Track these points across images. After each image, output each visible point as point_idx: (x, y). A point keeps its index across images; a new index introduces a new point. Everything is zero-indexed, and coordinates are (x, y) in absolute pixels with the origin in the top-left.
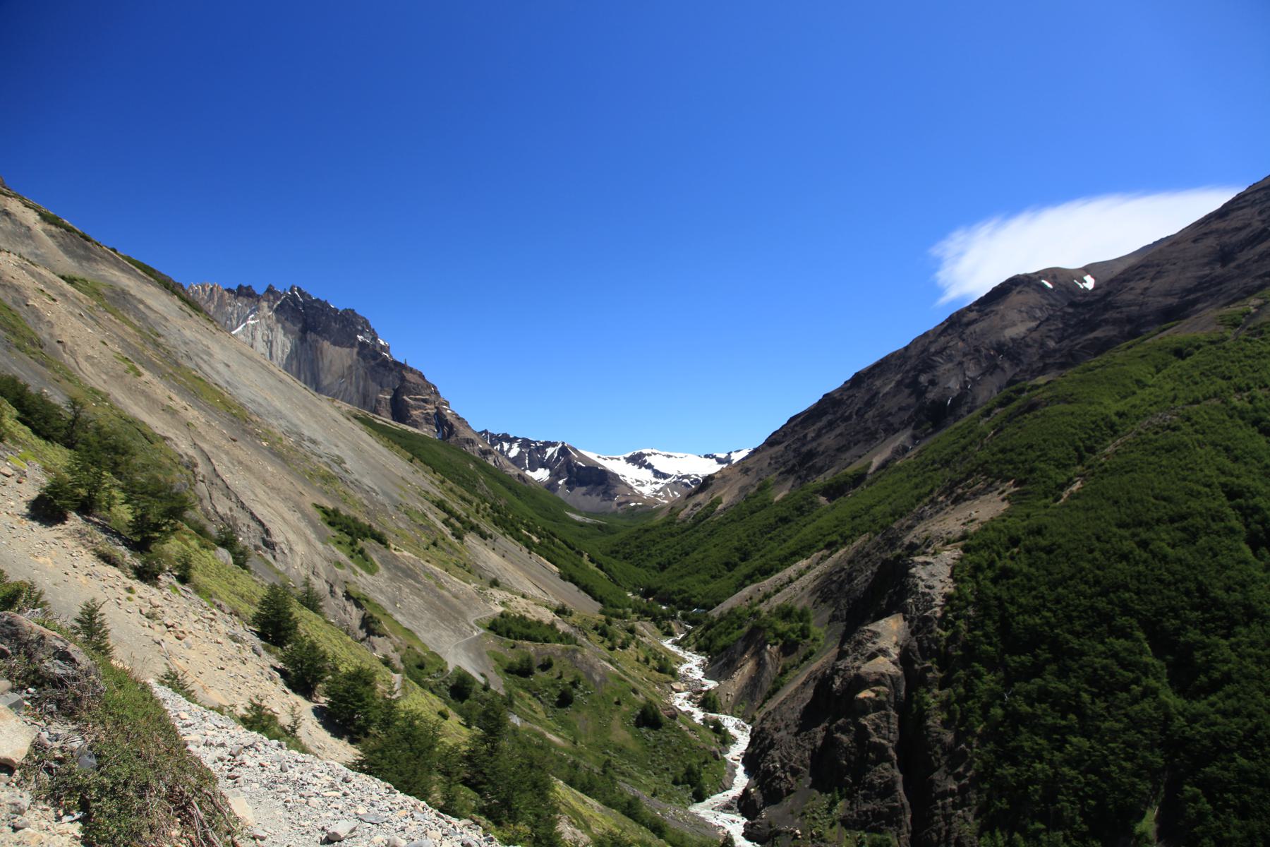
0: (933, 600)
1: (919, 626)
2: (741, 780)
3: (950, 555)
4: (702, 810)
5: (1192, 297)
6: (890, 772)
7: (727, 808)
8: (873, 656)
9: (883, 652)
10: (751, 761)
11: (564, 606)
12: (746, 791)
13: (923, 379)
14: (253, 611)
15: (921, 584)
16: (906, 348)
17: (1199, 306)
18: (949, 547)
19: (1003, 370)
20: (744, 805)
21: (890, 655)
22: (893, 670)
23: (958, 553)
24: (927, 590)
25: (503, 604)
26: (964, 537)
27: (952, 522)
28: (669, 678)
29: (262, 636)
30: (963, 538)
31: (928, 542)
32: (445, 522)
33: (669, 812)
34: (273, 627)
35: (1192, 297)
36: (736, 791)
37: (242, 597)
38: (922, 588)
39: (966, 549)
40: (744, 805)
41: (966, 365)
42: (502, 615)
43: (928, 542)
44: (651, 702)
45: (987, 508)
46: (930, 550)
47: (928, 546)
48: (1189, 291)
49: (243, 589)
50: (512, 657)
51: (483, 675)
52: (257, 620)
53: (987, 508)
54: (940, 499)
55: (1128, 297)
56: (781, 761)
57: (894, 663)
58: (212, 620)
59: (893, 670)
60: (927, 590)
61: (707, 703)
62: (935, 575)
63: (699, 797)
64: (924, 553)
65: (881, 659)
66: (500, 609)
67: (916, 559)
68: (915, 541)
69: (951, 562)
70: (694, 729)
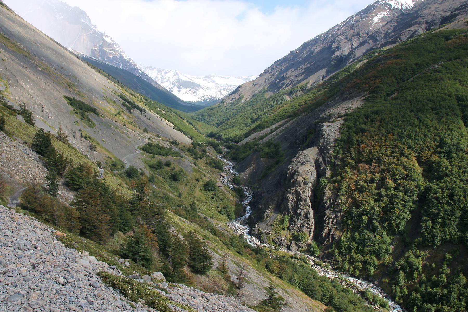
3: (340, 122)
5: (456, 12)
11: (175, 141)
13: (334, 46)
14: (31, 141)
16: (328, 32)
17: (459, 17)
19: (369, 43)
23: (342, 122)
24: (328, 137)
25: (149, 139)
26: (346, 115)
27: (341, 109)
28: (220, 171)
30: (345, 116)
31: (330, 117)
32: (124, 104)
35: (456, 12)
41: (353, 40)
42: (148, 144)
43: (330, 117)
45: (356, 104)
46: (331, 120)
47: (330, 119)
48: (456, 10)
50: (153, 161)
51: (141, 169)
53: (356, 104)
54: (337, 98)
55: (427, 11)
62: (331, 131)
64: (328, 122)
66: (147, 141)
67: (325, 123)
68: (325, 116)
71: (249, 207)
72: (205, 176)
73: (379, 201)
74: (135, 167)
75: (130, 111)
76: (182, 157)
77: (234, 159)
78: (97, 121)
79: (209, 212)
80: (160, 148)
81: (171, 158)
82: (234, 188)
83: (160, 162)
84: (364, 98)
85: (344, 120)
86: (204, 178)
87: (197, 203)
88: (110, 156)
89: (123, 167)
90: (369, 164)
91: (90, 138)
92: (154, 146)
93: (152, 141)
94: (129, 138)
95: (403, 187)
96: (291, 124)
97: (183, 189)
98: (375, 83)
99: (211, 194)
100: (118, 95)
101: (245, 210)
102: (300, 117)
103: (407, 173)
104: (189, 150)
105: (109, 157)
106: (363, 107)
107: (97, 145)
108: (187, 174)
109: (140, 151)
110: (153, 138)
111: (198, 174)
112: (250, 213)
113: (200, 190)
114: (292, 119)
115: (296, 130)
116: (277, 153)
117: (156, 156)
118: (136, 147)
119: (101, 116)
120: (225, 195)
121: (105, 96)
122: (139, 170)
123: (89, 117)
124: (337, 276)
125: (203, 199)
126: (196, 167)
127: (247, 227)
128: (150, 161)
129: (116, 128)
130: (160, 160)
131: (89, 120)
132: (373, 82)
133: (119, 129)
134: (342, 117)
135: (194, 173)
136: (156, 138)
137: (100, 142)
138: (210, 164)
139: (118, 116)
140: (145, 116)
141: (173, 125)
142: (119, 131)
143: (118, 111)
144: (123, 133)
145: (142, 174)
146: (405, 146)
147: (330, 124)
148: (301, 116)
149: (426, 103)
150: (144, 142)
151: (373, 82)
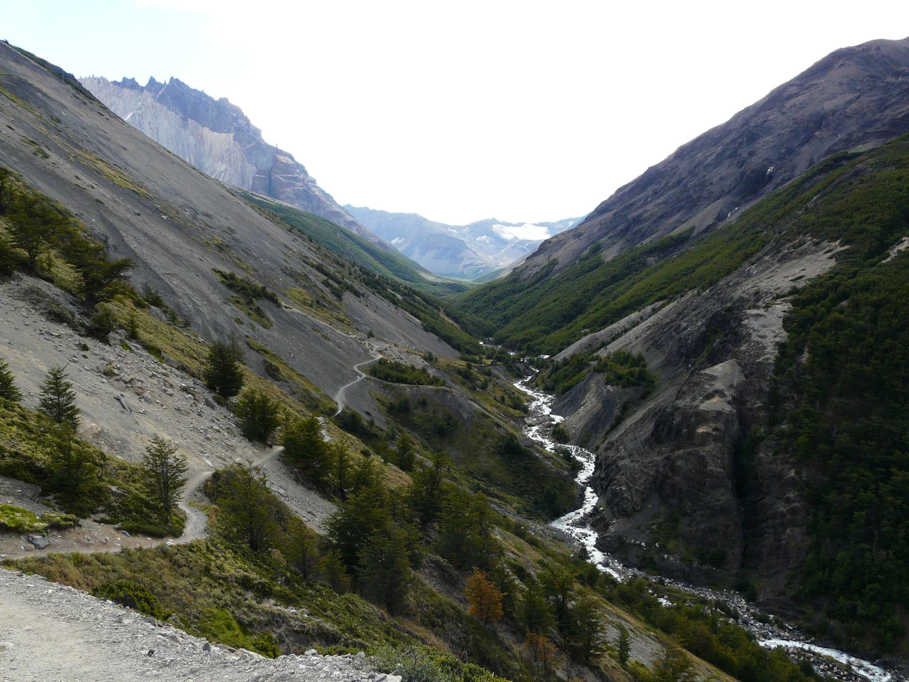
0: (764, 348)
1: (751, 370)
2: (591, 500)
3: (781, 308)
4: (562, 525)
6: (723, 496)
7: (582, 523)
8: (709, 397)
11: (430, 354)
12: (595, 508)
15: (754, 334)
18: (778, 301)
20: (595, 520)
22: (728, 408)
23: (787, 306)
24: (759, 340)
25: (380, 352)
26: (794, 291)
29: (211, 387)
30: (790, 293)
32: (326, 284)
34: (221, 379)
36: (588, 507)
37: (182, 351)
38: (754, 337)
40: (595, 520)
45: (815, 265)
46: (760, 303)
47: (758, 300)
49: (180, 345)
51: (368, 413)
54: (766, 258)
56: (627, 484)
57: (729, 403)
58: (165, 375)
59: (728, 408)
60: (759, 340)
61: (559, 434)
62: (767, 328)
63: (557, 514)
65: (716, 399)
67: (748, 312)
68: (744, 295)
69: (782, 314)
70: (548, 457)
72: (498, 425)
85: (792, 302)
89: (334, 410)
96: (666, 316)
100: (312, 266)
101: (582, 497)
102: (683, 299)
106: (834, 273)
114: (668, 304)
115: (680, 326)
134: (784, 296)
147: (761, 311)
148: (687, 297)
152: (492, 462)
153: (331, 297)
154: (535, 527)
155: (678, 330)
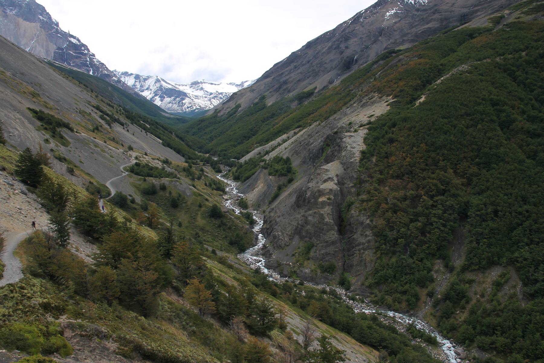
0: (354, 154)
1: (346, 166)
2: (262, 241)
3: (363, 132)
6: (333, 235)
8: (325, 181)
9: (330, 179)
10: (266, 232)
11: (167, 159)
12: (264, 245)
14: (13, 168)
15: (349, 147)
18: (361, 128)
21: (334, 180)
22: (335, 187)
23: (366, 131)
25: (136, 158)
26: (370, 123)
27: (363, 115)
28: (221, 193)
32: (102, 117)
33: (231, 258)
36: (260, 245)
38: (349, 148)
39: (369, 129)
40: (265, 252)
42: (137, 164)
44: (216, 205)
45: (380, 109)
46: (352, 129)
47: (351, 128)
50: (144, 186)
51: (130, 196)
52: (17, 173)
54: (355, 105)
56: (281, 231)
57: (336, 184)
59: (335, 187)
61: (242, 204)
62: (355, 143)
63: (242, 250)
64: (349, 131)
66: (135, 161)
67: (346, 134)
70: (237, 218)
71: (261, 235)
72: (207, 200)
73: (416, 221)
74: (124, 193)
75: (109, 125)
76: (179, 178)
77: (236, 179)
78: (71, 138)
79: (216, 243)
80: (151, 169)
81: (165, 181)
82: (241, 213)
83: (153, 186)
84: (387, 103)
85: (368, 129)
86: (207, 203)
87: (200, 233)
88: (92, 181)
89: (109, 194)
90: (401, 179)
91: (65, 159)
92: (144, 167)
93: (140, 160)
94: (113, 157)
95: (442, 204)
96: (302, 136)
97: (183, 217)
98: (398, 87)
99: (217, 222)
100: (94, 107)
101: (257, 239)
102: (311, 127)
103: (444, 188)
104: (184, 170)
105: (90, 182)
106: (389, 113)
107: (74, 167)
108: (186, 198)
109: (127, 173)
110: (140, 157)
111: (199, 198)
112: (263, 242)
113: (203, 218)
114: (302, 130)
115: (309, 142)
116: (289, 170)
117: (147, 178)
118: (121, 168)
119: (77, 132)
120: (233, 222)
121: (78, 107)
122: (129, 197)
123: (61, 133)
124: (374, 311)
125: (208, 228)
126: (195, 190)
127: (262, 259)
128: (140, 185)
129: (96, 146)
130: (153, 184)
131: (62, 137)
132: (396, 85)
133: (98, 147)
134: (364, 125)
135: (194, 196)
136: (144, 156)
137: (78, 164)
138: (210, 185)
139: (96, 131)
140: (128, 131)
141: (161, 141)
142: (99, 149)
143: (95, 126)
144: (104, 151)
145: (133, 201)
146: (441, 158)
147: (352, 134)
148: (313, 126)
149: (459, 108)
150: (131, 162)
151: (396, 85)
152: (204, 222)
153: (106, 126)
154: (231, 258)
155: (308, 144)
